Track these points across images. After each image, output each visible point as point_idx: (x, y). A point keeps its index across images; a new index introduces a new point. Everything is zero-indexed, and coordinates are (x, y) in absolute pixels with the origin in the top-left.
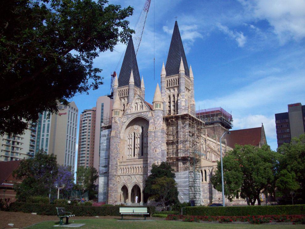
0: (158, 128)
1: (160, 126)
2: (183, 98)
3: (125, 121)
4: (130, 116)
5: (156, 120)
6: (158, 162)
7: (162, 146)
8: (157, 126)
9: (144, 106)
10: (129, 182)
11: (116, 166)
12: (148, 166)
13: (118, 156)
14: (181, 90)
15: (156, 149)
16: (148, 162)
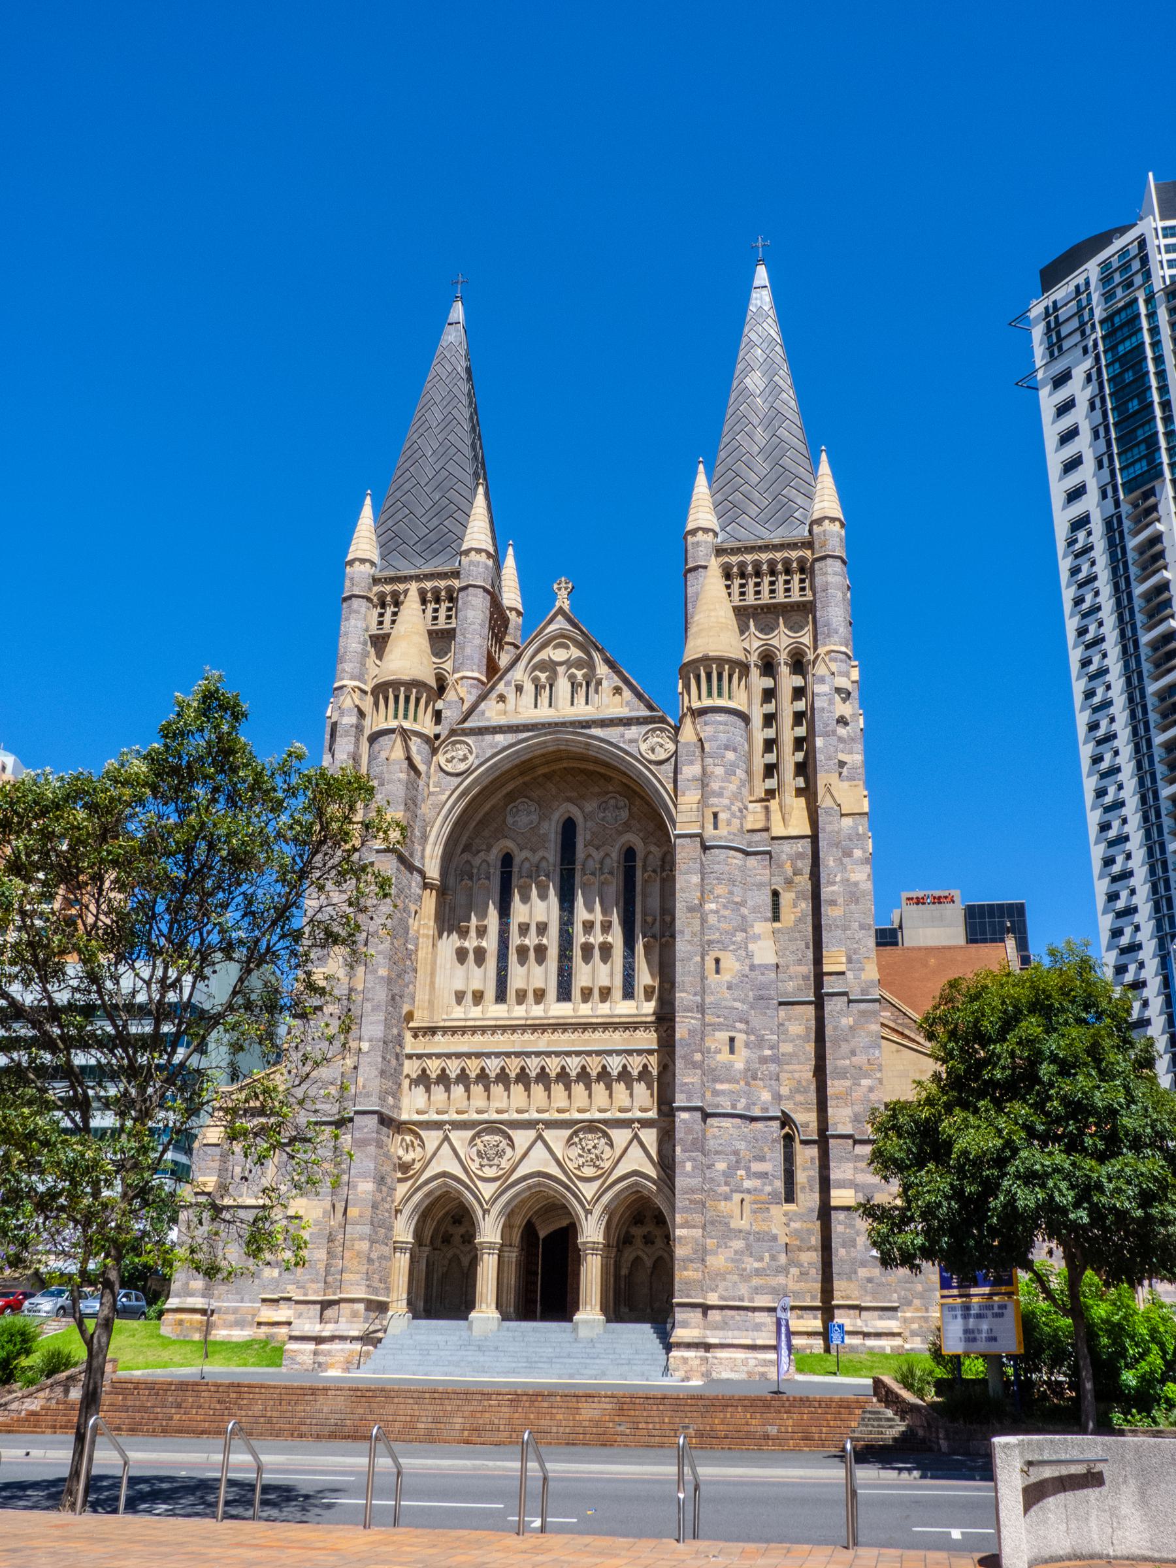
0: (729, 824)
1: (740, 811)
2: (842, 674)
3: (462, 767)
4: (501, 739)
5: (719, 771)
6: (732, 1040)
7: (757, 937)
8: (729, 809)
9: (605, 683)
10: (490, 1172)
11: (397, 1056)
12: (679, 1063)
13: (411, 986)
14: (827, 624)
15: (720, 955)
16: (680, 1032)
